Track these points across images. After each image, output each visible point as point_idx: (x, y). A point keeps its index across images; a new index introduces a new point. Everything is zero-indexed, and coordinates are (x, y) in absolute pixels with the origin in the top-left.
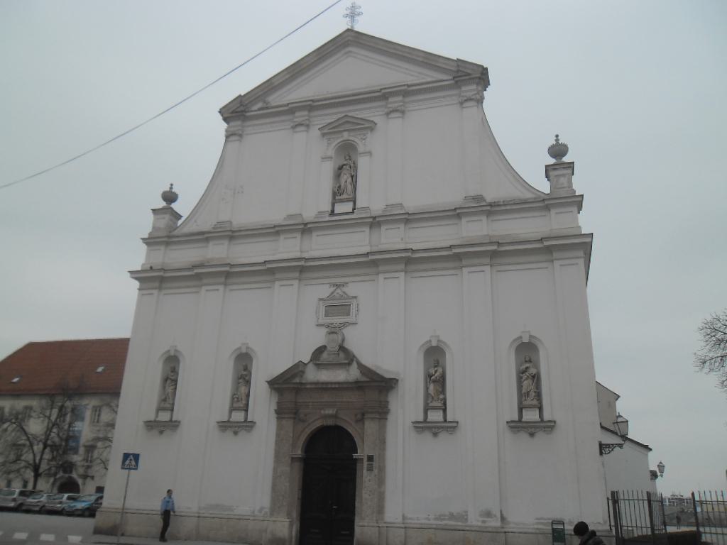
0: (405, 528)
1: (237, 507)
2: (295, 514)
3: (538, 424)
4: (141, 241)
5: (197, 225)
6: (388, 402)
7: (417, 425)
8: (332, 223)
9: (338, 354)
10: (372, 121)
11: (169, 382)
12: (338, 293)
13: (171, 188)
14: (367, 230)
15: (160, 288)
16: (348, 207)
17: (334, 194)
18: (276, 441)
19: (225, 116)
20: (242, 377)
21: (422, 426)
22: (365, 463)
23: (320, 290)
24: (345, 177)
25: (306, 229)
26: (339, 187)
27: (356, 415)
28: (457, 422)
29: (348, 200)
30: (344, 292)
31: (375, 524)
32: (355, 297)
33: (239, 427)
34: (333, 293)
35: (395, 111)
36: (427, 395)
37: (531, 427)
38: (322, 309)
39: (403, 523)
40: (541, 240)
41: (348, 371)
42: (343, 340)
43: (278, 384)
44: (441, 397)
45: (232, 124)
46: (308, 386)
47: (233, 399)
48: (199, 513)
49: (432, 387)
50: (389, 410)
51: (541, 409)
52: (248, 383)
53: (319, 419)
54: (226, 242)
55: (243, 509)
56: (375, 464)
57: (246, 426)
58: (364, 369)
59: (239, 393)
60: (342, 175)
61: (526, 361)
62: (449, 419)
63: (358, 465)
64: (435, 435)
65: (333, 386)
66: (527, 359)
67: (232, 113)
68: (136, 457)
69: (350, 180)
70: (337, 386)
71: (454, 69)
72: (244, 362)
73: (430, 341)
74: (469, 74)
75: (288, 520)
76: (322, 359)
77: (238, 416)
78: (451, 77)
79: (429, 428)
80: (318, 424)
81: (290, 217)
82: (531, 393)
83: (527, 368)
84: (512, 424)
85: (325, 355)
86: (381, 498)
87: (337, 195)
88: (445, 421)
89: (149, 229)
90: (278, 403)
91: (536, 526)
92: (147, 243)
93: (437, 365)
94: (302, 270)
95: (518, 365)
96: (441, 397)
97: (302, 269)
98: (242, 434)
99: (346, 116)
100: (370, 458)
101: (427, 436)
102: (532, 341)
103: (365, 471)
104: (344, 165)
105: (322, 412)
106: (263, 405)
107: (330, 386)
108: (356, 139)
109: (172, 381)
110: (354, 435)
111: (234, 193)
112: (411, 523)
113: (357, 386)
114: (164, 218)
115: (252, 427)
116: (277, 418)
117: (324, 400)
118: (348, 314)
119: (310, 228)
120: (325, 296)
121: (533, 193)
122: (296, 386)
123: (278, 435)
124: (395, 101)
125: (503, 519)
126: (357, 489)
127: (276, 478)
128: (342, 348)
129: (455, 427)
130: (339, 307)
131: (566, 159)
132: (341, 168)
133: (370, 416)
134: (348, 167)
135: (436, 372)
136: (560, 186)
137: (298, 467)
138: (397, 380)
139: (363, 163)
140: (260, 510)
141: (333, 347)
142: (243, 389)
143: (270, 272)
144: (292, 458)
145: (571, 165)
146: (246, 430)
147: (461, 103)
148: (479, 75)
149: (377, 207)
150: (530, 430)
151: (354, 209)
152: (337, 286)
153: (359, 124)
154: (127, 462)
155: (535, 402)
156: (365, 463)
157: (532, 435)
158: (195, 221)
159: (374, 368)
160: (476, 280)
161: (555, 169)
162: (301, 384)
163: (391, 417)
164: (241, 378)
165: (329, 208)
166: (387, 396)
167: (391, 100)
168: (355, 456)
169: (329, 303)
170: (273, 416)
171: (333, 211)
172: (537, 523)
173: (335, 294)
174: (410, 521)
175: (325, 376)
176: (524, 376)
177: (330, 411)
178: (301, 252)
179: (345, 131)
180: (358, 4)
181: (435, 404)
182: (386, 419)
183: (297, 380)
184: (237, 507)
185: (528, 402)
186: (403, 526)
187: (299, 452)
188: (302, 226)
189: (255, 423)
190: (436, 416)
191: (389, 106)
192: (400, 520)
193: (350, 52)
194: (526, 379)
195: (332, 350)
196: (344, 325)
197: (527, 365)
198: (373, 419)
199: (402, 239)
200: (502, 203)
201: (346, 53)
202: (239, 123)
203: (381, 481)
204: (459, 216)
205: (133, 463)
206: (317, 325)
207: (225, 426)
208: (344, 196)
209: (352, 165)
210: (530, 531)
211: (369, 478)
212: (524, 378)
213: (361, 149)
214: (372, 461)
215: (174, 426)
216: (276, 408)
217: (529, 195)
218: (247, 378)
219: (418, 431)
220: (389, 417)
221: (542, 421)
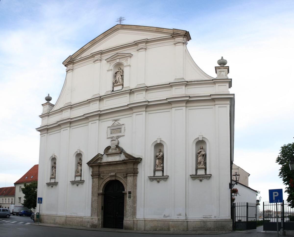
0: (145, 221)
6: (138, 168)
7: (150, 178)
8: (113, 94)
9: (116, 149)
10: (131, 54)
12: (116, 124)
14: (128, 95)
16: (120, 88)
17: (114, 84)
18: (92, 187)
20: (79, 163)
21: (152, 179)
22: (128, 195)
23: (108, 123)
24: (118, 76)
26: (116, 81)
27: (124, 175)
29: (119, 85)
30: (119, 123)
31: (132, 219)
33: (78, 183)
34: (114, 124)
39: (144, 219)
41: (120, 156)
42: (118, 143)
43: (91, 164)
46: (103, 164)
52: (81, 165)
53: (109, 177)
58: (127, 155)
59: (78, 170)
60: (117, 76)
64: (158, 182)
65: (114, 163)
69: (120, 77)
70: (115, 163)
72: (79, 155)
75: (97, 218)
76: (109, 152)
77: (78, 179)
79: (156, 179)
80: (108, 179)
82: (202, 162)
87: (115, 83)
90: (92, 172)
93: (160, 151)
94: (100, 115)
98: (80, 185)
100: (130, 193)
101: (155, 182)
102: (203, 140)
103: (127, 198)
104: (118, 72)
105: (110, 174)
107: (112, 163)
108: (123, 61)
110: (123, 183)
113: (123, 162)
115: (83, 182)
116: (92, 178)
117: (110, 170)
118: (121, 132)
119: (102, 98)
120: (110, 125)
122: (98, 164)
123: (92, 185)
126: (125, 205)
127: (92, 202)
128: (117, 146)
133: (129, 175)
137: (100, 197)
138: (142, 159)
141: (113, 147)
142: (79, 168)
144: (98, 194)
146: (81, 184)
149: (133, 86)
152: (116, 120)
156: (128, 195)
162: (100, 163)
164: (78, 164)
166: (137, 166)
168: (123, 192)
169: (112, 128)
170: (91, 177)
173: (115, 124)
177: (113, 174)
178: (99, 109)
182: (137, 176)
183: (99, 161)
188: (99, 98)
189: (84, 181)
190: (159, 174)
196: (118, 137)
203: (135, 202)
206: (107, 138)
208: (119, 83)
212: (199, 156)
214: (131, 194)
216: (91, 174)
218: (81, 163)
219: (151, 181)
220: (138, 175)
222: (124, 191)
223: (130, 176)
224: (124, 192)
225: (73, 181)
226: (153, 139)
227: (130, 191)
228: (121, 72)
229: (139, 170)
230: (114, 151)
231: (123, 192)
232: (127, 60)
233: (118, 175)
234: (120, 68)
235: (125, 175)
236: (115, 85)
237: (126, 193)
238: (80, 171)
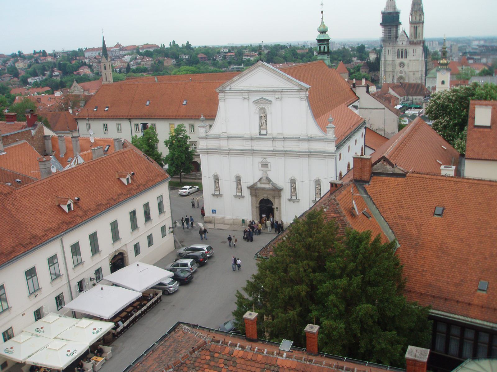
11: (216, 183)
17: (260, 127)
21: (290, 200)
22: (276, 209)
23: (258, 159)
25: (252, 139)
32: (269, 163)
38: (260, 165)
49: (293, 190)
52: (241, 184)
63: (274, 209)
64: (294, 202)
69: (264, 122)
72: (239, 181)
74: (303, 89)
77: (239, 194)
85: (262, 180)
97: (253, 153)
99: (262, 98)
100: (277, 208)
101: (292, 203)
106: (246, 193)
124: (278, 95)
130: (265, 165)
132: (261, 117)
139: (269, 116)
141: (264, 178)
142: (239, 186)
143: (243, 153)
152: (264, 158)
156: (276, 209)
160: (305, 161)
170: (250, 195)
171: (260, 132)
175: (263, 186)
187: (258, 205)
203: (280, 213)
207: (236, 196)
213: (267, 112)
226: (290, 177)
230: (264, 182)
233: (269, 196)
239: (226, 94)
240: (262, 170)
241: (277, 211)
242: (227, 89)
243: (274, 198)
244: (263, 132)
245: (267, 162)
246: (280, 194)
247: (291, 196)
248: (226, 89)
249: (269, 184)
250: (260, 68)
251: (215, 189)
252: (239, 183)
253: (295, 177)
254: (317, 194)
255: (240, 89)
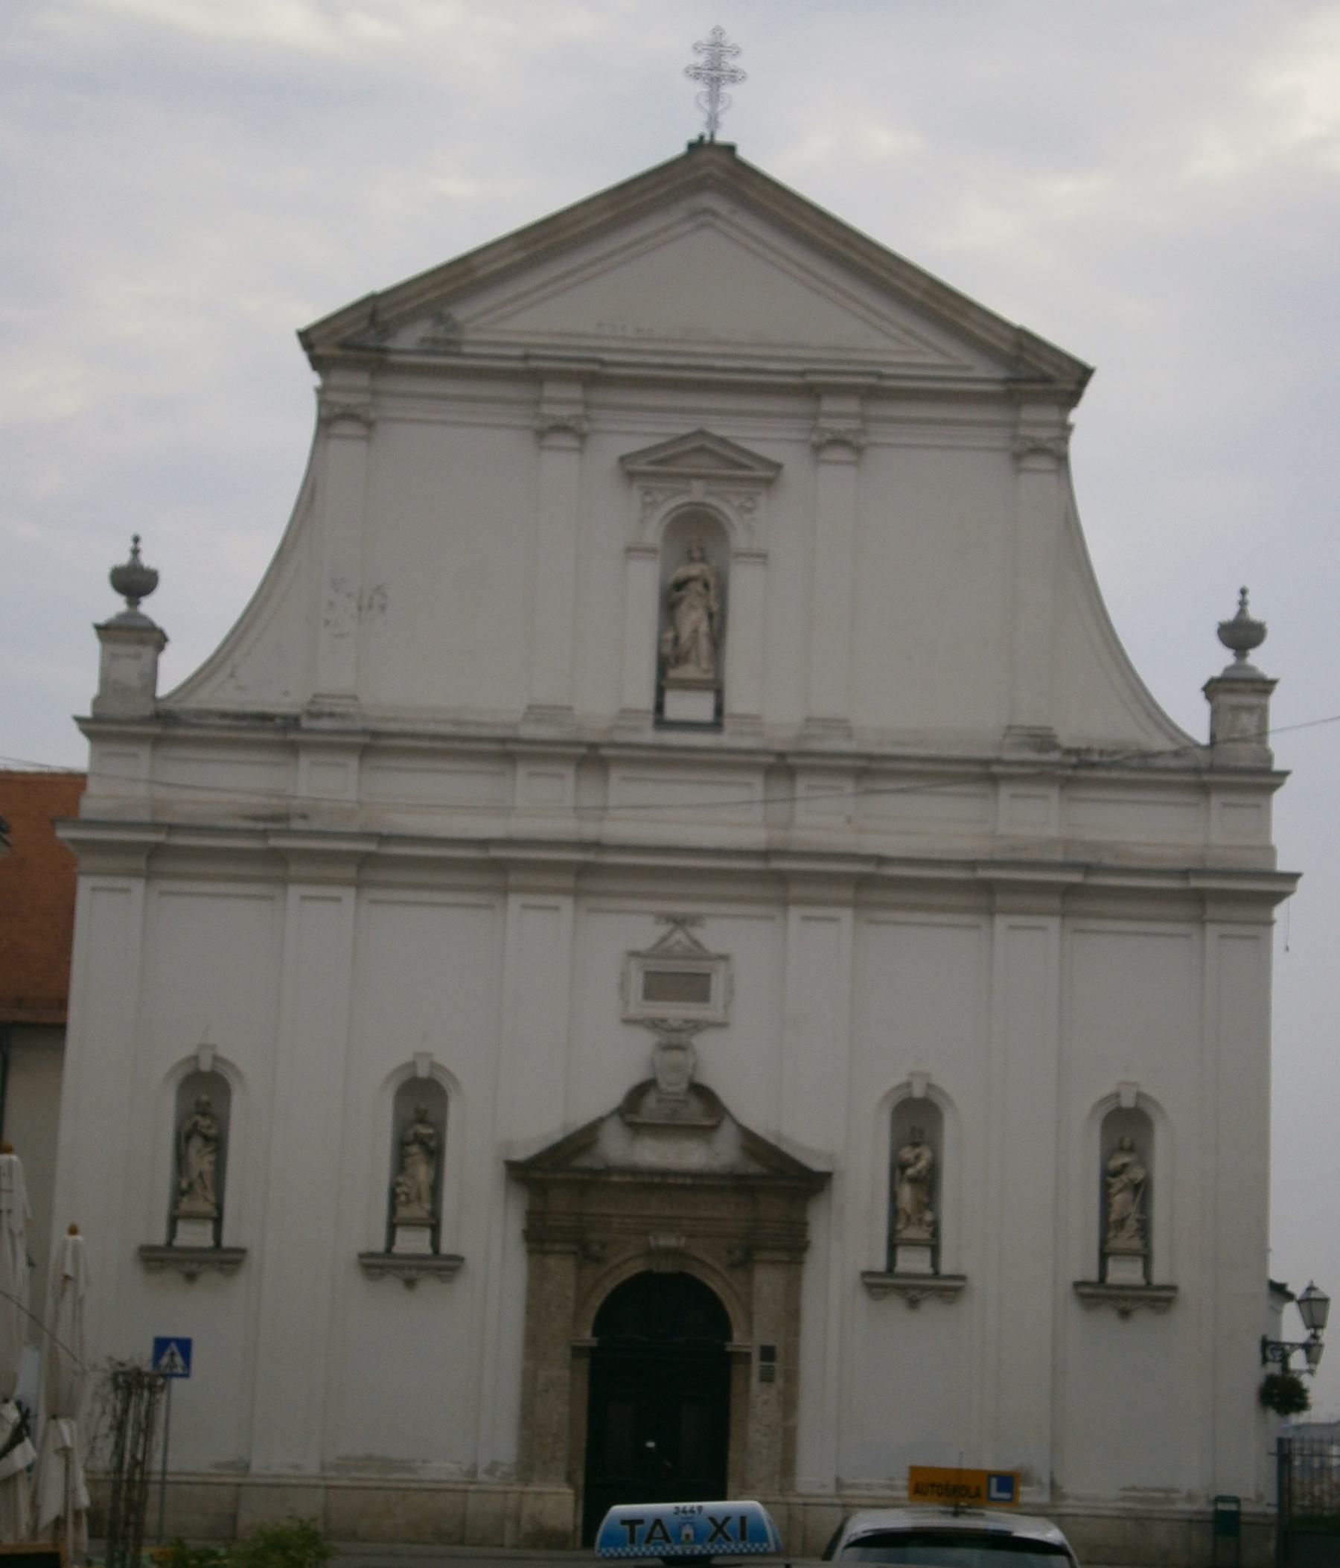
0: (844, 1506)
1: (424, 1461)
2: (580, 1478)
3: (1141, 1293)
4: (74, 726)
5: (241, 688)
12: (679, 942)
13: (136, 552)
15: (149, 876)
17: (663, 664)
19: (319, 350)
22: (756, 1364)
28: (962, 1278)
30: (695, 942)
31: (780, 1499)
32: (724, 958)
33: (420, 1268)
34: (664, 939)
35: (838, 442)
36: (894, 1212)
37: (1126, 1298)
40: (1185, 874)
42: (695, 1067)
44: (928, 1217)
45: (339, 378)
46: (615, 1179)
47: (393, 1196)
48: (324, 1478)
49: (906, 1192)
50: (809, 1242)
51: (1147, 1258)
52: (435, 1154)
54: (353, 762)
55: (443, 1468)
56: (778, 1365)
57: (440, 1269)
58: (753, 1144)
60: (684, 606)
61: (1122, 1149)
62: (946, 1268)
65: (680, 1181)
66: (1127, 1143)
67: (345, 345)
68: (185, 1346)
69: (704, 627)
70: (689, 1181)
71: (1005, 347)
73: (909, 1085)
74: (1047, 380)
77: (413, 1242)
78: (1001, 374)
79: (901, 1289)
80: (636, 1267)
81: (536, 712)
83: (1125, 1166)
84: (1087, 1290)
85: (650, 1101)
86: (789, 1438)
88: (936, 1274)
89: (93, 688)
91: (1121, 1505)
92: (88, 734)
95: (1107, 1155)
96: (928, 1217)
100: (768, 1353)
101: (894, 1307)
103: (755, 1383)
107: (671, 1181)
108: (726, 505)
109: (207, 1139)
111: (360, 608)
112: (853, 1497)
114: (137, 656)
116: (530, 1252)
120: (644, 944)
121: (1172, 739)
125: (1054, 1487)
129: (957, 1289)
131: (1258, 659)
132: (680, 585)
134: (698, 587)
135: (918, 1157)
136: (1237, 735)
137: (584, 1363)
140: (490, 1471)
141: (673, 1085)
142: (423, 1173)
145: (1265, 686)
147: (1017, 457)
148: (1071, 387)
150: (1123, 1304)
151: (719, 710)
152: (679, 922)
153: (741, 466)
154: (165, 1360)
155: (1136, 1243)
156: (756, 1364)
157: (1125, 1314)
158: (232, 675)
159: (772, 1140)
161: (1231, 691)
163: (813, 1261)
165: (646, 700)
167: (828, 405)
168: (730, 1348)
169: (654, 965)
171: (659, 707)
172: (1123, 1499)
173: (671, 941)
174: (848, 1492)
176: (1117, 1183)
177: (666, 1241)
179: (699, 477)
180: (731, 38)
181: (912, 1233)
183: (584, 1162)
184: (424, 1461)
185: (1121, 1241)
186: (837, 1501)
187: (587, 1337)
191: (824, 423)
192: (831, 1489)
193: (707, 211)
194: (1120, 1191)
195: (670, 1089)
196: (696, 1026)
197: (1124, 1159)
198: (774, 1263)
199: (849, 821)
200: (1095, 758)
201: (695, 214)
202: (362, 380)
203: (789, 1403)
204: (994, 780)
205: (179, 1360)
208: (687, 671)
209: (712, 581)
210: (1108, 1513)
211: (765, 1397)
213: (739, 540)
215: (230, 1262)
217: (1159, 743)
221: (1149, 1285)
222: (728, 1336)
223: (774, 1263)
224: (734, 1349)
225: (372, 1255)
227: (769, 1342)
228: (706, 585)
229: (817, 1233)
231: (729, 1349)
232: (749, 504)
234: (702, 550)
235: (738, 1254)
236: (674, 674)
237: (748, 1355)
238: (426, 1194)
239: (388, 383)
240: (654, 1024)
241: (767, 1377)
242: (408, 339)
243: (744, 1262)
244: (679, 706)
245: (697, 953)
246: (804, 1224)
247: (892, 1247)
248: (390, 344)
249: (703, 1132)
250: (708, 200)
251: (175, 1204)
252: (421, 1140)
253: (940, 1082)
254: (1121, 1223)
255: (518, 352)
